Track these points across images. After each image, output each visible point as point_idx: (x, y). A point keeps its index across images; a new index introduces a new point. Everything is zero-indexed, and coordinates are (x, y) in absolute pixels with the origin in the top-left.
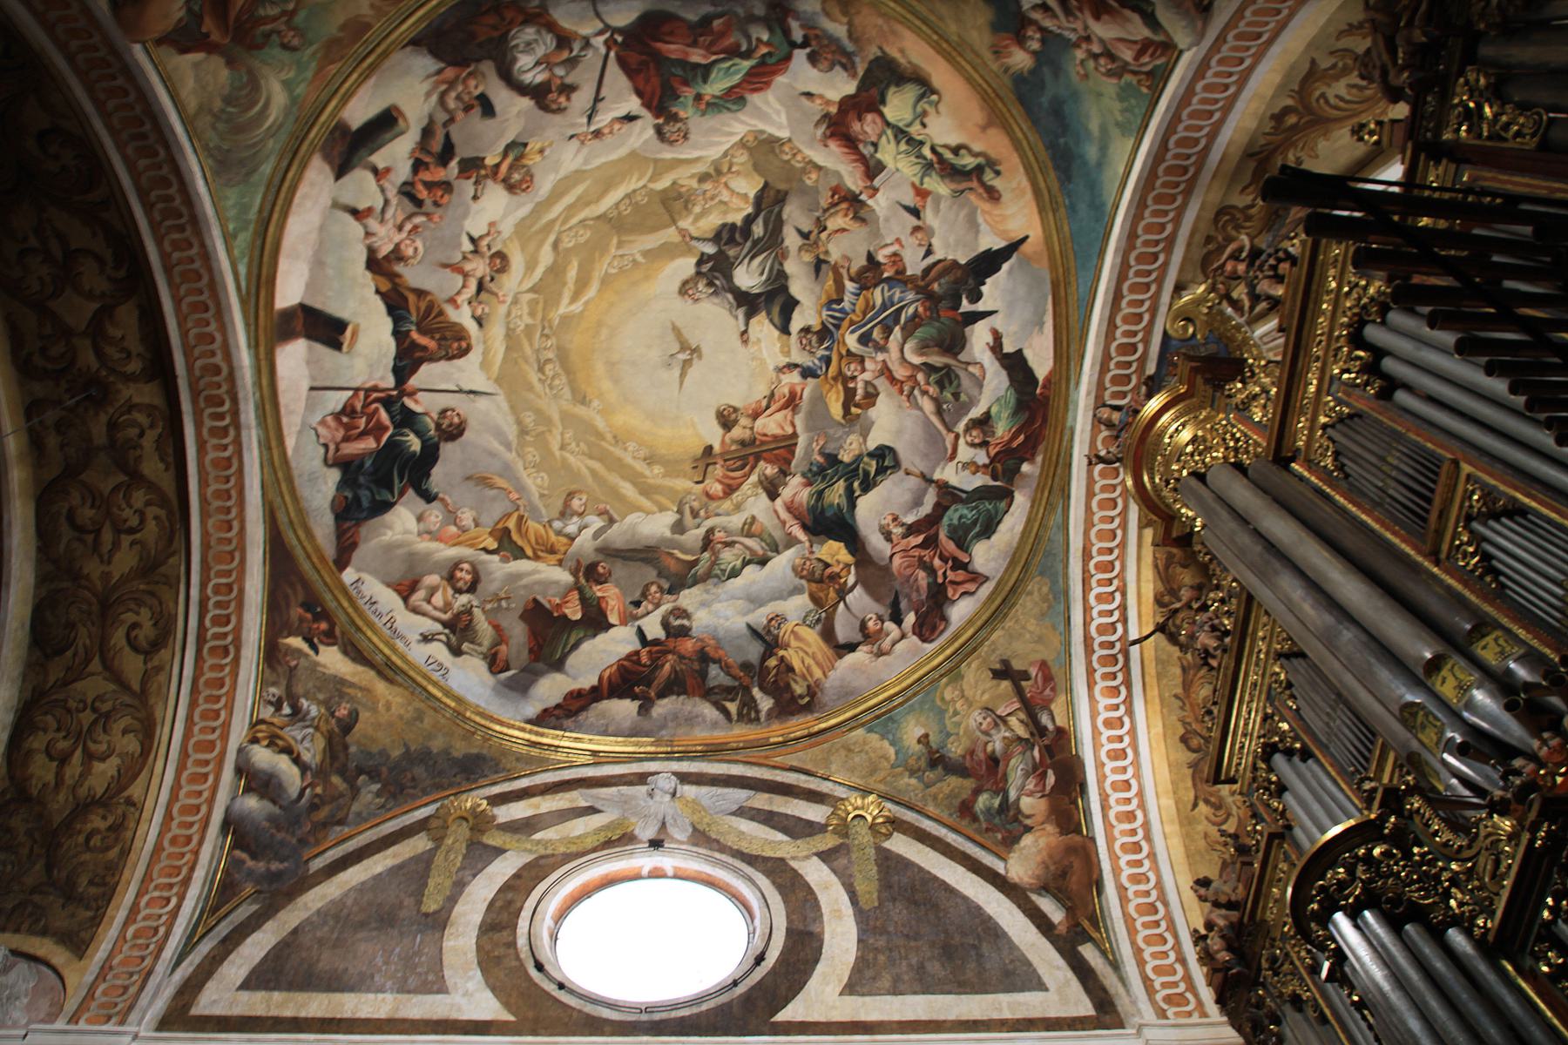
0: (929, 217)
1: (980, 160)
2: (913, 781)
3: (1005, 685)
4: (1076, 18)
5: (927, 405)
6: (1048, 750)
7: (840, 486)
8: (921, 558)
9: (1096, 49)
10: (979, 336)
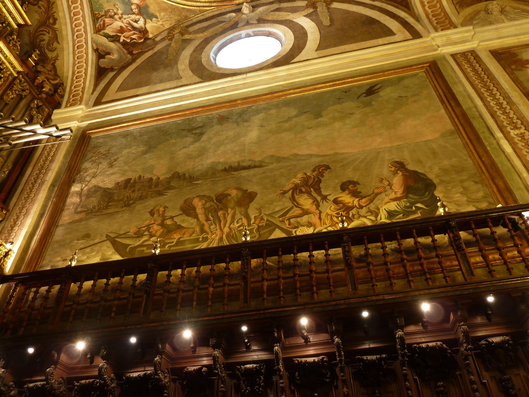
4: (127, 23)
9: (116, 17)
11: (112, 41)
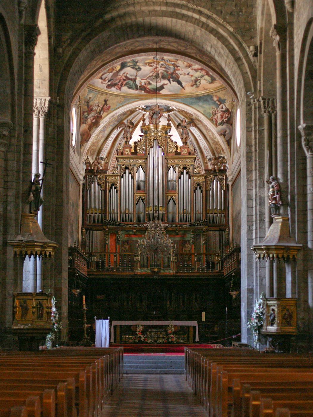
0: (187, 76)
1: (198, 85)
2: (84, 102)
3: (104, 103)
5: (151, 74)
6: (98, 117)
7: (132, 64)
8: (121, 80)
9: (216, 112)
10: (166, 82)
11: (223, 125)
